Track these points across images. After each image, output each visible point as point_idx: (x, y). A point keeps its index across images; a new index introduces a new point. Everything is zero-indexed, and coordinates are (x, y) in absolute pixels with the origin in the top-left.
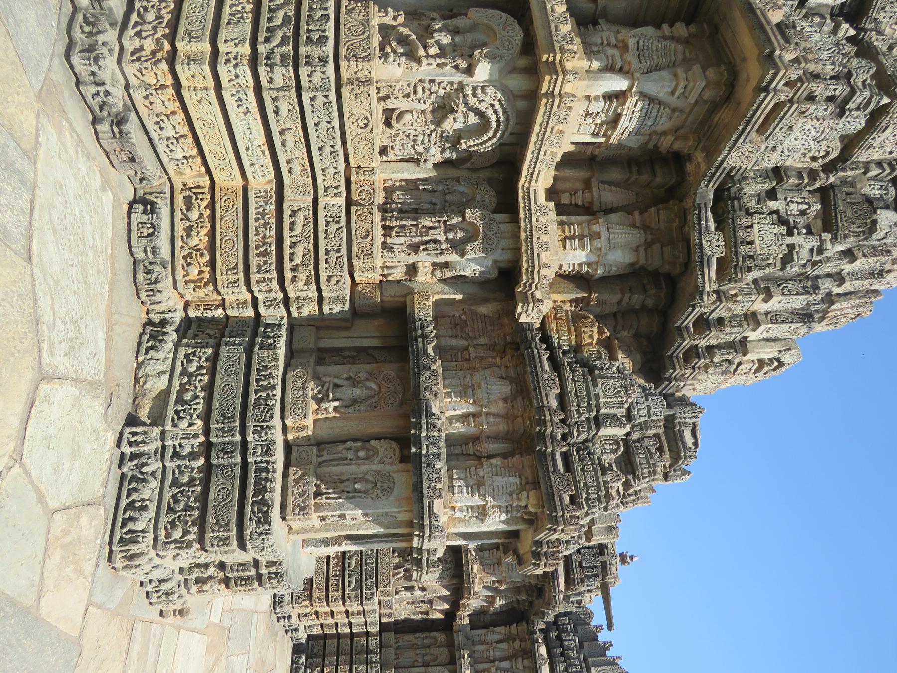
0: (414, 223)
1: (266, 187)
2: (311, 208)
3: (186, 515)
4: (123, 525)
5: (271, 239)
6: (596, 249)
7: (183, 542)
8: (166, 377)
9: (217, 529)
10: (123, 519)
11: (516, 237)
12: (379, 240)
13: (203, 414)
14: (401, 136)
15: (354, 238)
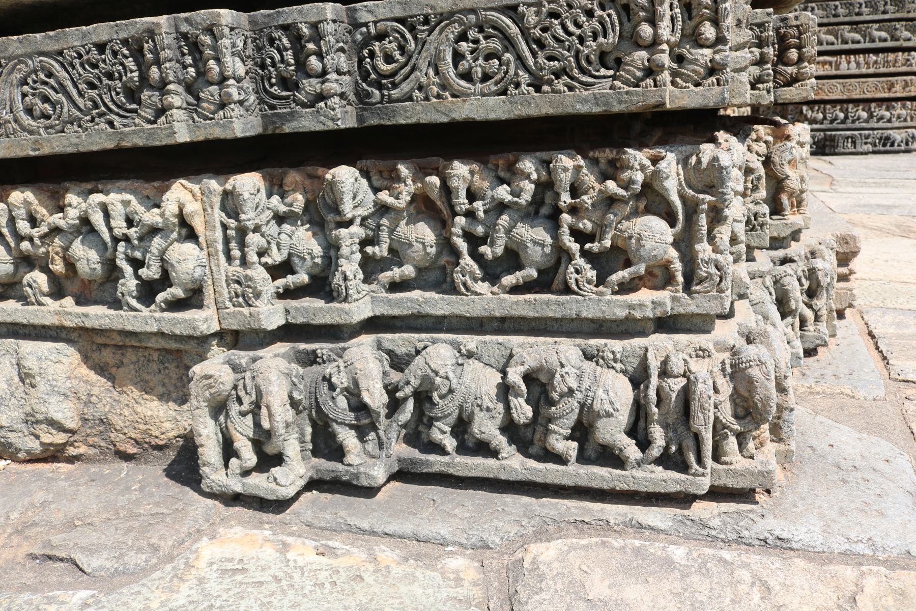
3: (573, 210)
4: (610, 457)
7: (691, 209)
8: (33, 351)
9: (641, 55)
10: (583, 458)
13: (148, 188)
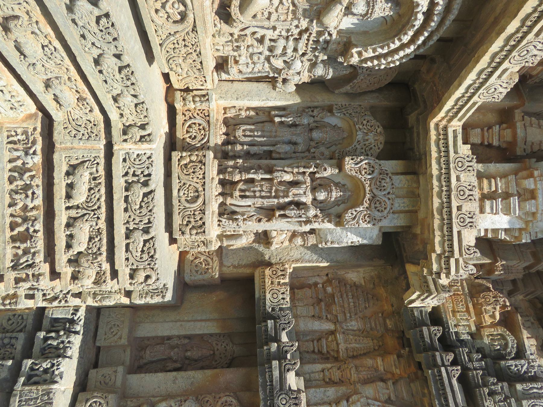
0: (268, 176)
1: (25, 125)
2: (102, 161)
5: (34, 213)
6: (527, 214)
11: (417, 196)
12: (214, 207)
14: (250, 40)
15: (175, 202)
